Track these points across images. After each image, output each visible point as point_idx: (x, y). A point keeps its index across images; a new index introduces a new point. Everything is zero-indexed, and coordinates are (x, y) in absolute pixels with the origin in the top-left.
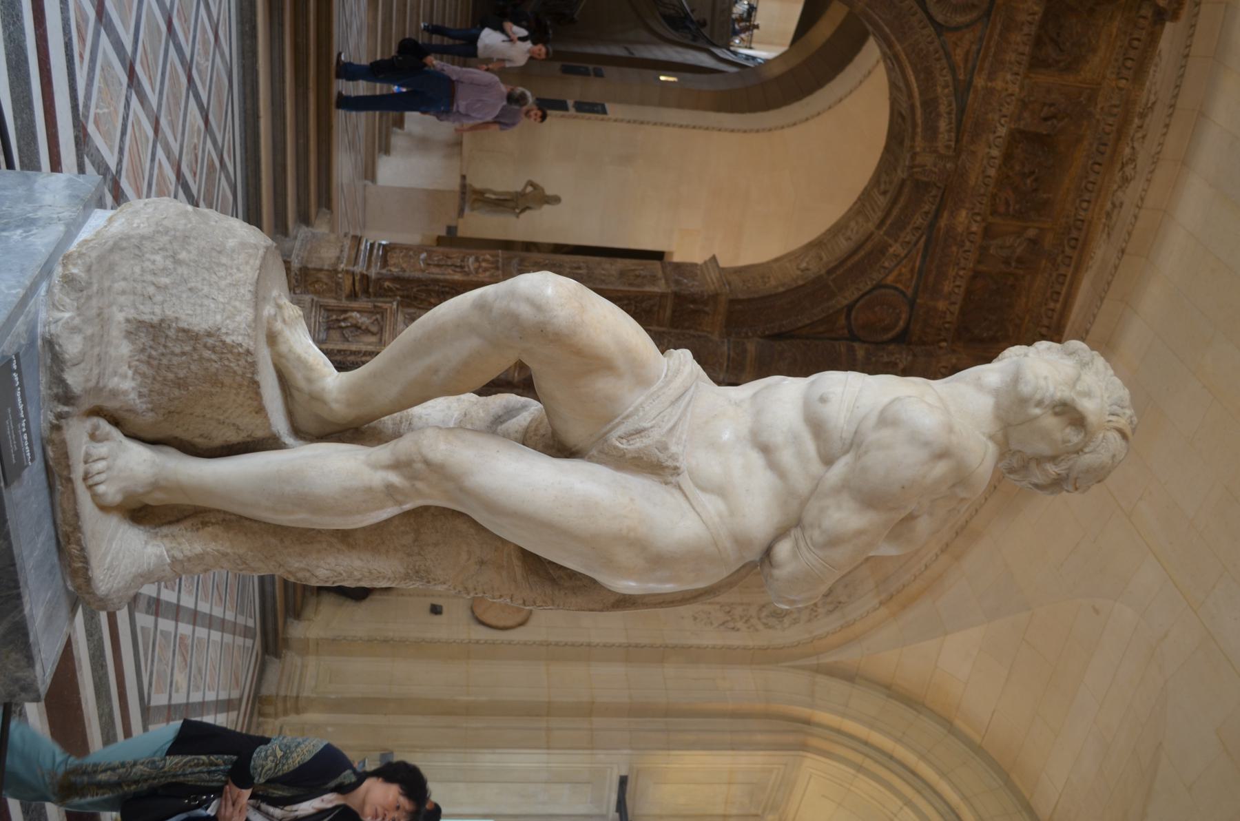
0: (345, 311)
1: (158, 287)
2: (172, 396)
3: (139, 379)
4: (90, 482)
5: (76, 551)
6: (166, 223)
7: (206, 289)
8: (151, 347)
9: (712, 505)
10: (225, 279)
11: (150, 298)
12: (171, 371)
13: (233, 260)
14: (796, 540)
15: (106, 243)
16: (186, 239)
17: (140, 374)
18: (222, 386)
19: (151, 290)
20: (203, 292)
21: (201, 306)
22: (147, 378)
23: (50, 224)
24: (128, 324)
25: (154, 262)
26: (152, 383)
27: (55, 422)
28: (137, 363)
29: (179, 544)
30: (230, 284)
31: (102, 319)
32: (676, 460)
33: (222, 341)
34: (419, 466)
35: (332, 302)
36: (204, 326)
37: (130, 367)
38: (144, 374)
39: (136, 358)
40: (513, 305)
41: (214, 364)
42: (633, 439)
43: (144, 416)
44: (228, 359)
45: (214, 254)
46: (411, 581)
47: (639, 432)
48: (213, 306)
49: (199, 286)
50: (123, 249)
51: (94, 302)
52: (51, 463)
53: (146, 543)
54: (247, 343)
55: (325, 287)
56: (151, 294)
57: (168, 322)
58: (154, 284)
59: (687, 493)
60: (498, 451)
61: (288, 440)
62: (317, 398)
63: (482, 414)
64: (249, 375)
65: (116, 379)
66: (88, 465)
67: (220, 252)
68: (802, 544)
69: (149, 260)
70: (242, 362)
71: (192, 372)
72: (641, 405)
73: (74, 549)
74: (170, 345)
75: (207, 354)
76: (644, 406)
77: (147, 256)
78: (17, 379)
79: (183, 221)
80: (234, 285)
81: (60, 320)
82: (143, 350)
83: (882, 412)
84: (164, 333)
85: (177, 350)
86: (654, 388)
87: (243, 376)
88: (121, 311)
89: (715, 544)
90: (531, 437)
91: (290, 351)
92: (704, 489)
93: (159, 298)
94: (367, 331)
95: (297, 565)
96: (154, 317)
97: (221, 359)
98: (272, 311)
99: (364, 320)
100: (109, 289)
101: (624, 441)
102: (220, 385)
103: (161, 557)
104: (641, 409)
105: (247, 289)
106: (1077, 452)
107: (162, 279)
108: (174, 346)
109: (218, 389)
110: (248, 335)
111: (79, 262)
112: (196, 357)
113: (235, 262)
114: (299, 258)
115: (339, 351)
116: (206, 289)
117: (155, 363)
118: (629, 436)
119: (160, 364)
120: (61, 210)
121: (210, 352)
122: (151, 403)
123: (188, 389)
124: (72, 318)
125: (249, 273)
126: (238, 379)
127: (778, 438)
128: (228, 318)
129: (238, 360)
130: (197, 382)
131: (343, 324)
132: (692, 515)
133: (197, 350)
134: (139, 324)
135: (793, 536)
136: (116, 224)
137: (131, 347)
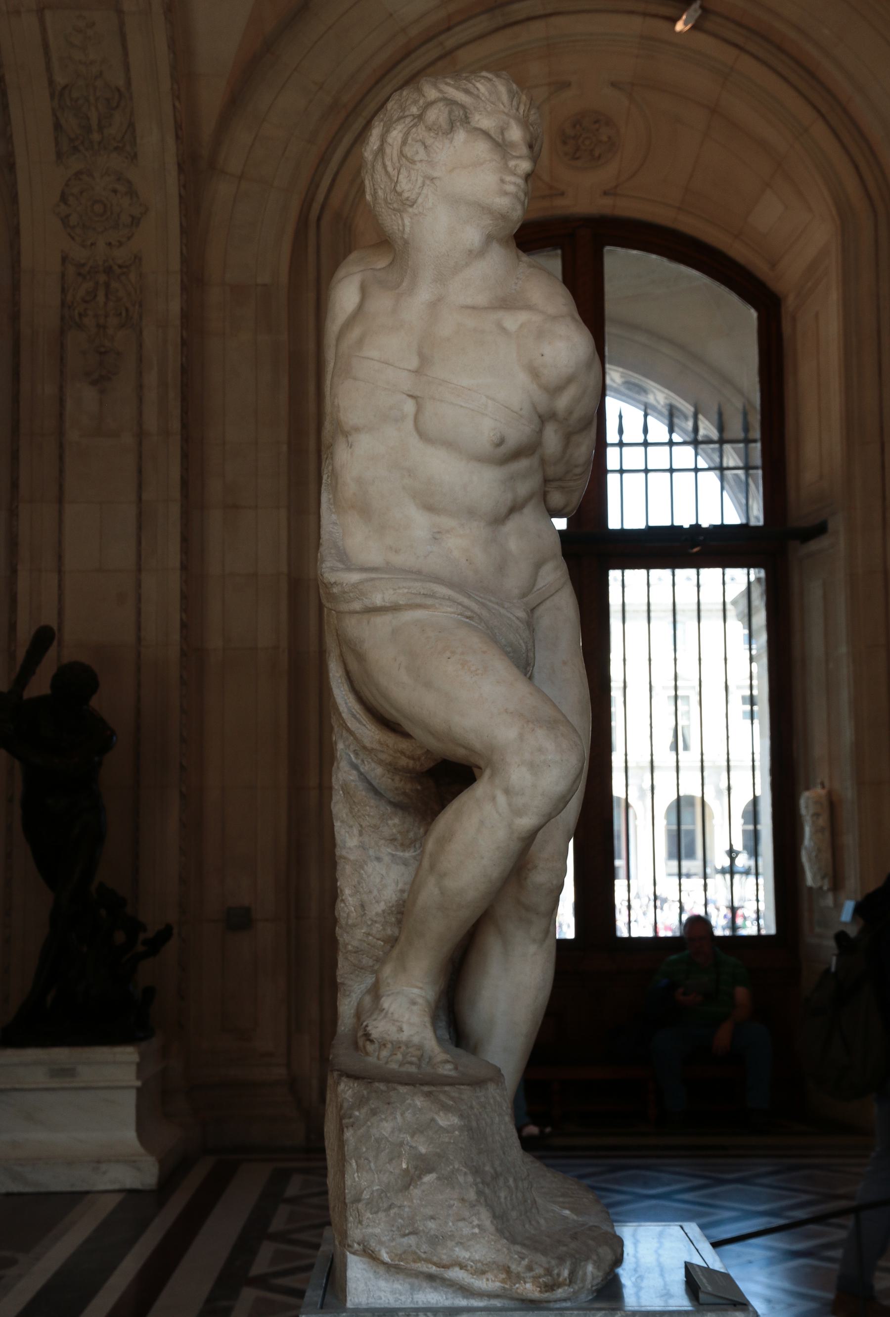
6: (472, 1195)
59: (540, 602)
63: (396, 821)
79: (461, 1179)
111: (556, 1272)
116: (497, 1138)
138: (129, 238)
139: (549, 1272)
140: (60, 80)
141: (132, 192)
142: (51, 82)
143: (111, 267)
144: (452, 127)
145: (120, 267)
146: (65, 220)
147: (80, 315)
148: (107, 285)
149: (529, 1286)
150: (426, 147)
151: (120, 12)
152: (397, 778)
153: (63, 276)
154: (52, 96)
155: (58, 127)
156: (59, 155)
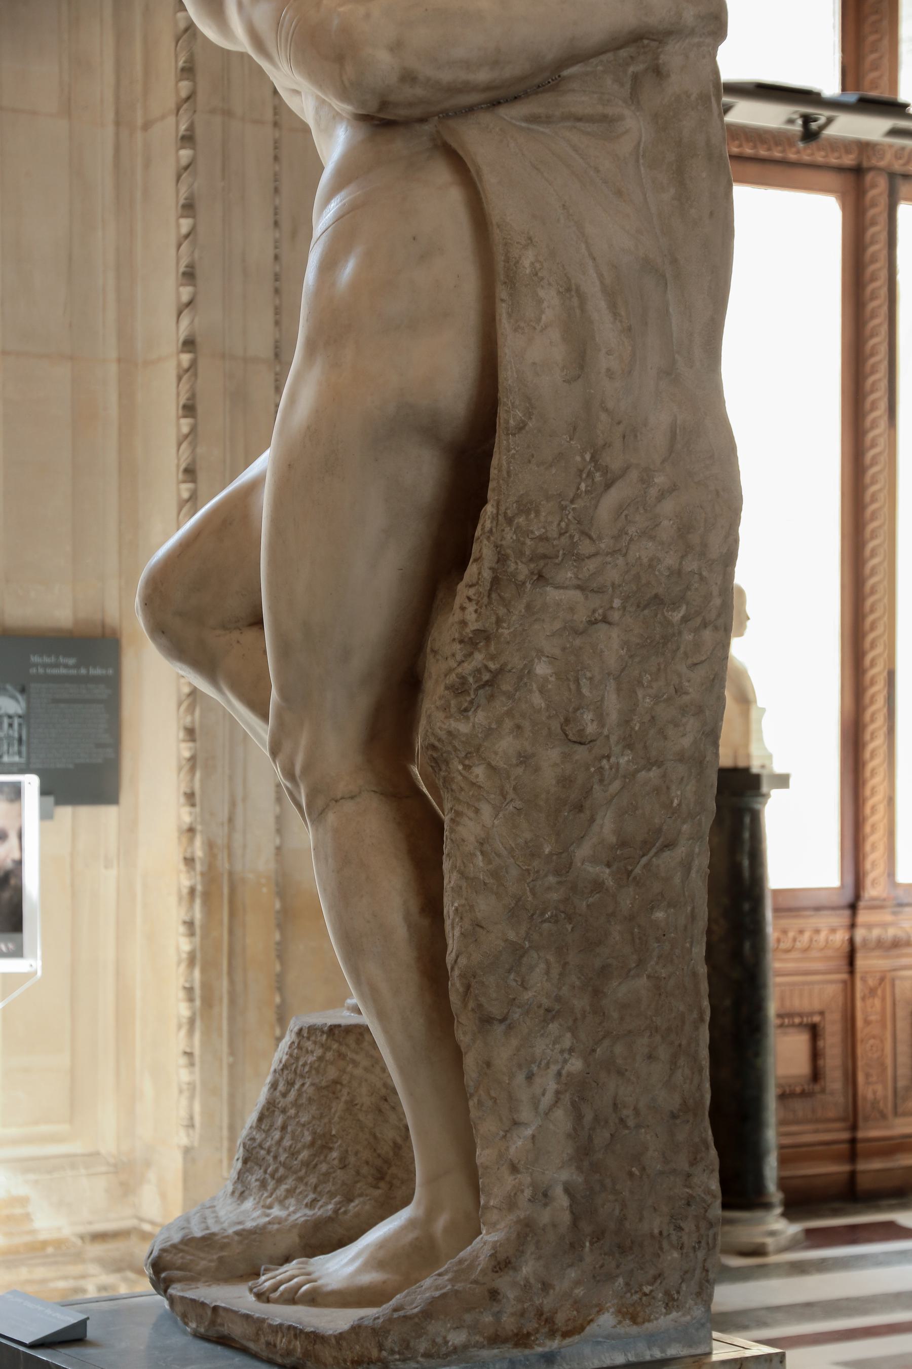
2: (336, 1162)
3: (292, 1201)
12: (299, 1152)
17: (286, 1198)
18: (341, 1084)
22: (296, 1188)
26: (306, 1184)
38: (288, 1191)
41: (307, 1086)
43: (345, 1212)
44: (304, 1065)
46: (453, 779)
57: (246, 1140)
64: (325, 1037)
70: (309, 1045)
71: (309, 1123)
74: (268, 1144)
84: (255, 1148)
85: (277, 1135)
87: (326, 1048)
97: (302, 1076)
102: (339, 1087)
108: (272, 1139)
109: (345, 1091)
112: (292, 1112)
117: (282, 1171)
119: (284, 1165)
122: (332, 1195)
123: (334, 1135)
126: (329, 1055)
129: (307, 1052)
130: (326, 1120)
133: (285, 1109)
134: (240, 1181)
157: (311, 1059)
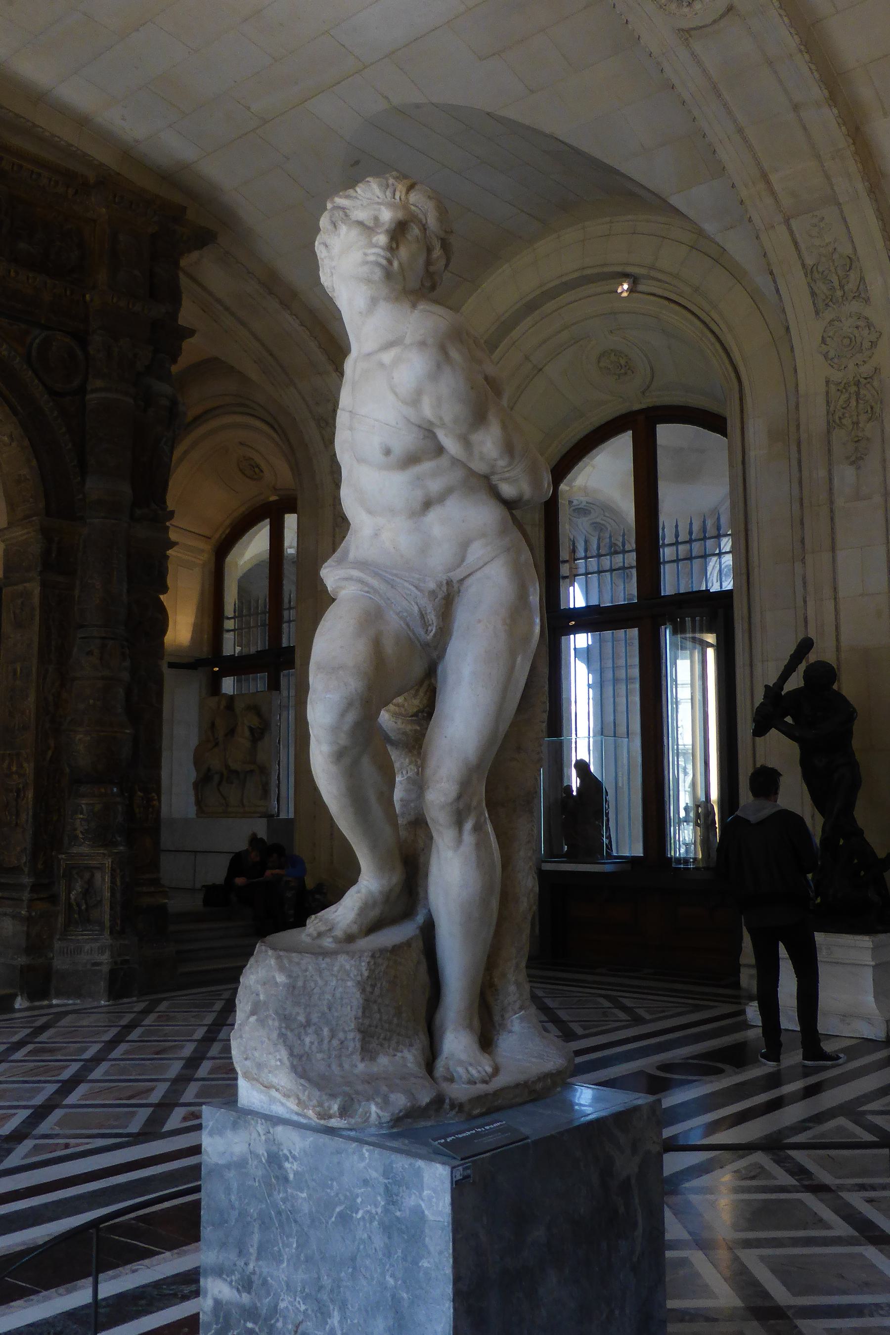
0: (70, 905)
1: (333, 1037)
4: (488, 1079)
5: (541, 1085)
6: (275, 1035)
7: (328, 996)
8: (378, 1038)
9: (477, 552)
10: (316, 982)
11: (342, 1043)
13: (298, 976)
14: (501, 480)
15: (302, 1085)
16: (286, 1019)
19: (335, 1042)
20: (330, 998)
21: (342, 999)
23: (274, 1140)
24: (365, 1059)
25: (312, 1043)
27: (457, 1109)
28: (391, 1049)
29: (509, 1004)
30: (320, 976)
31: (370, 1079)
32: (441, 582)
33: (367, 980)
34: (461, 805)
35: (61, 919)
36: (358, 995)
37: (395, 1055)
39: (388, 1050)
40: (346, 727)
42: (428, 621)
45: (296, 992)
47: (422, 616)
48: (340, 990)
49: (325, 1002)
50: (305, 1071)
51: (360, 1088)
52: (484, 1110)
53: (510, 1032)
54: (366, 958)
55: (46, 928)
56: (338, 1042)
58: (330, 1041)
60: (446, 737)
61: (420, 919)
62: (387, 898)
65: (409, 1065)
66: (477, 1081)
67: (294, 987)
68: (507, 475)
69: (310, 1048)
72: (398, 614)
73: (539, 1086)
74: (375, 1022)
75: (377, 991)
76: (398, 611)
77: (307, 1049)
78: (451, 1138)
79: (270, 1022)
80: (321, 972)
81: (376, 1112)
82: (381, 1045)
83: (405, 402)
85: (378, 1016)
86: (382, 603)
88: (356, 1066)
89: (508, 550)
90: (405, 710)
91: (355, 923)
92: (463, 560)
93: (341, 1035)
94: (90, 882)
95: (526, 904)
96: (357, 1039)
98: (330, 940)
99: (78, 887)
100: (342, 1077)
101: (430, 628)
103: (522, 1019)
104: (401, 614)
105: (322, 962)
106: (425, 229)
107: (325, 1033)
110: (360, 957)
111: (326, 1104)
112: (380, 1000)
113: (300, 973)
114: (16, 957)
115: (112, 908)
116: (328, 996)
117: (388, 1034)
118: (425, 625)
120: (255, 1135)
121: (376, 989)
124: (377, 1104)
125: (308, 962)
127: (419, 494)
128: (348, 975)
131: (83, 907)
132: (487, 570)
135: (496, 482)
136: (275, 1081)
137: (381, 1055)
138: (870, 357)
139: (320, 1104)
140: (810, 262)
141: (869, 325)
142: (804, 266)
143: (859, 381)
144: (335, 226)
145: (866, 378)
146: (826, 356)
147: (840, 418)
148: (858, 394)
149: (311, 1111)
150: (326, 246)
151: (839, 204)
152: (399, 721)
153: (827, 393)
154: (806, 276)
155: (813, 294)
156: (817, 313)
157: (383, 968)
